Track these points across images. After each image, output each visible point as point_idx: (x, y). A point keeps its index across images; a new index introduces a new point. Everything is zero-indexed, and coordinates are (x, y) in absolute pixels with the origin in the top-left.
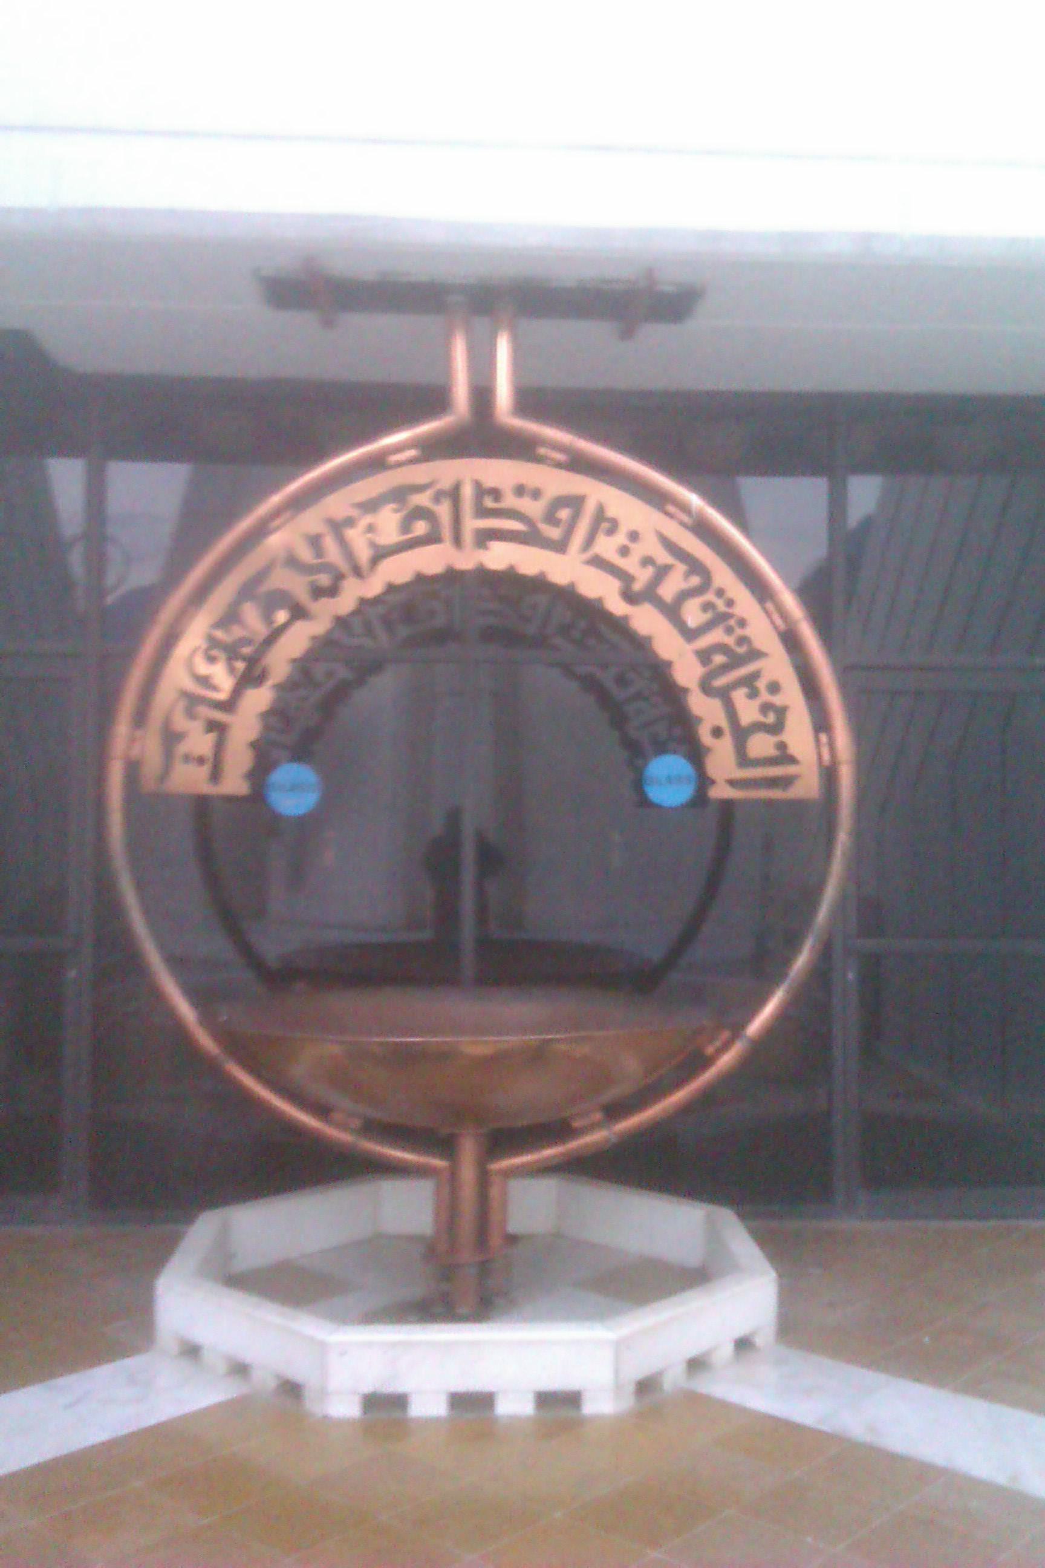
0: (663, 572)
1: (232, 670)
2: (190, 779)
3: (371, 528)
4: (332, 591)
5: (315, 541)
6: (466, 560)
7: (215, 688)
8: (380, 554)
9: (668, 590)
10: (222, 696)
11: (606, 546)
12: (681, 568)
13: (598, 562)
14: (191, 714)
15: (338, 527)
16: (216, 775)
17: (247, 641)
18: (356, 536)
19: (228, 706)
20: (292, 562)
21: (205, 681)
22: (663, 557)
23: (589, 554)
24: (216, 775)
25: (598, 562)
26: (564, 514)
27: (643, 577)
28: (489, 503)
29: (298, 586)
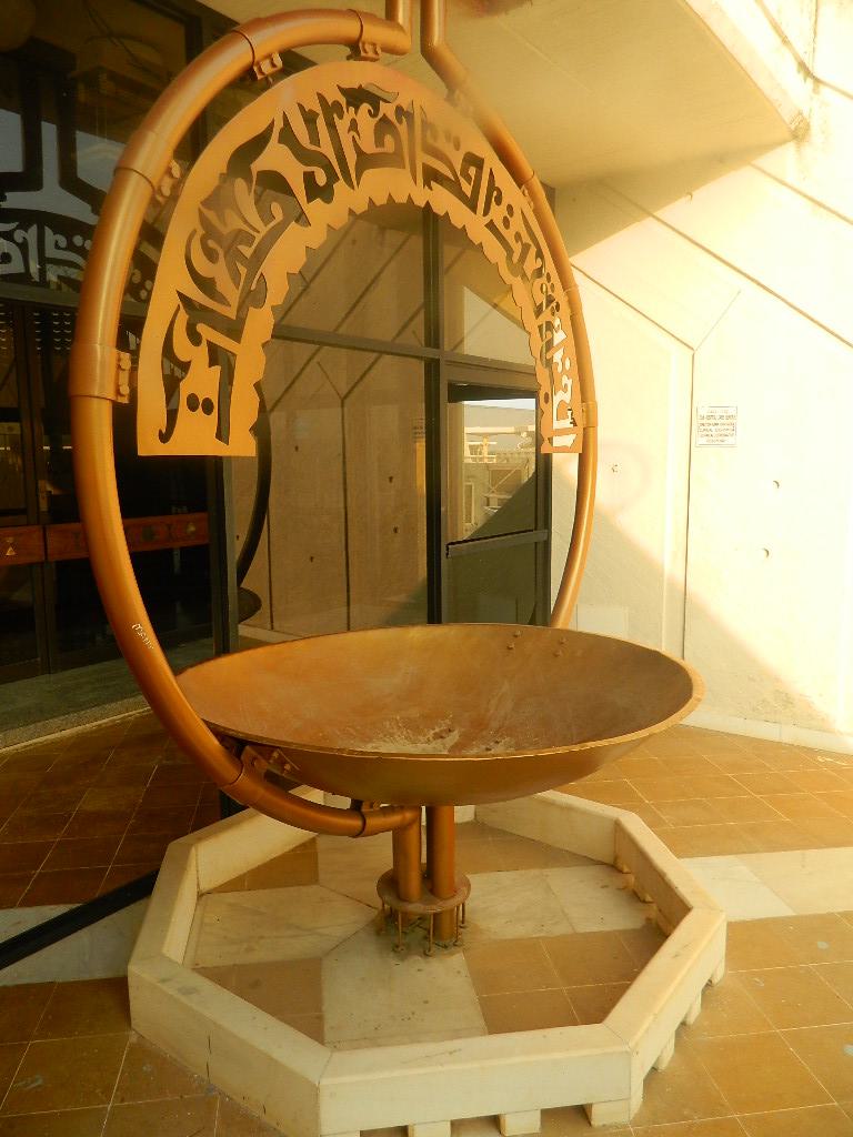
0: (526, 248)
1: (235, 276)
2: (194, 438)
3: (354, 126)
4: (326, 193)
5: (310, 119)
6: (421, 196)
7: (222, 300)
8: (365, 161)
9: (531, 264)
10: (231, 313)
11: (497, 213)
12: (533, 250)
13: (491, 226)
14: (195, 338)
15: (331, 110)
16: (222, 434)
17: (243, 237)
18: (342, 125)
19: (234, 330)
20: (287, 136)
21: (205, 284)
22: (526, 239)
23: (487, 220)
24: (222, 434)
25: (491, 226)
26: (472, 171)
27: (517, 248)
28: (430, 141)
29: (294, 172)
